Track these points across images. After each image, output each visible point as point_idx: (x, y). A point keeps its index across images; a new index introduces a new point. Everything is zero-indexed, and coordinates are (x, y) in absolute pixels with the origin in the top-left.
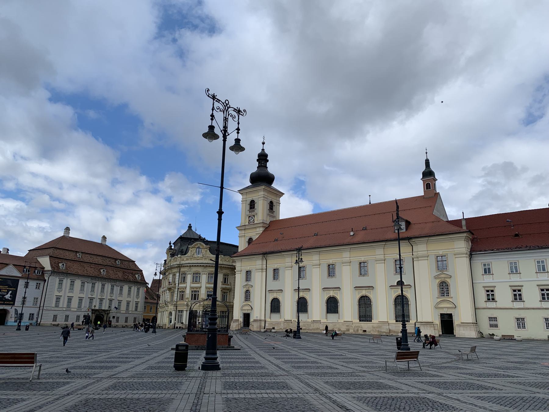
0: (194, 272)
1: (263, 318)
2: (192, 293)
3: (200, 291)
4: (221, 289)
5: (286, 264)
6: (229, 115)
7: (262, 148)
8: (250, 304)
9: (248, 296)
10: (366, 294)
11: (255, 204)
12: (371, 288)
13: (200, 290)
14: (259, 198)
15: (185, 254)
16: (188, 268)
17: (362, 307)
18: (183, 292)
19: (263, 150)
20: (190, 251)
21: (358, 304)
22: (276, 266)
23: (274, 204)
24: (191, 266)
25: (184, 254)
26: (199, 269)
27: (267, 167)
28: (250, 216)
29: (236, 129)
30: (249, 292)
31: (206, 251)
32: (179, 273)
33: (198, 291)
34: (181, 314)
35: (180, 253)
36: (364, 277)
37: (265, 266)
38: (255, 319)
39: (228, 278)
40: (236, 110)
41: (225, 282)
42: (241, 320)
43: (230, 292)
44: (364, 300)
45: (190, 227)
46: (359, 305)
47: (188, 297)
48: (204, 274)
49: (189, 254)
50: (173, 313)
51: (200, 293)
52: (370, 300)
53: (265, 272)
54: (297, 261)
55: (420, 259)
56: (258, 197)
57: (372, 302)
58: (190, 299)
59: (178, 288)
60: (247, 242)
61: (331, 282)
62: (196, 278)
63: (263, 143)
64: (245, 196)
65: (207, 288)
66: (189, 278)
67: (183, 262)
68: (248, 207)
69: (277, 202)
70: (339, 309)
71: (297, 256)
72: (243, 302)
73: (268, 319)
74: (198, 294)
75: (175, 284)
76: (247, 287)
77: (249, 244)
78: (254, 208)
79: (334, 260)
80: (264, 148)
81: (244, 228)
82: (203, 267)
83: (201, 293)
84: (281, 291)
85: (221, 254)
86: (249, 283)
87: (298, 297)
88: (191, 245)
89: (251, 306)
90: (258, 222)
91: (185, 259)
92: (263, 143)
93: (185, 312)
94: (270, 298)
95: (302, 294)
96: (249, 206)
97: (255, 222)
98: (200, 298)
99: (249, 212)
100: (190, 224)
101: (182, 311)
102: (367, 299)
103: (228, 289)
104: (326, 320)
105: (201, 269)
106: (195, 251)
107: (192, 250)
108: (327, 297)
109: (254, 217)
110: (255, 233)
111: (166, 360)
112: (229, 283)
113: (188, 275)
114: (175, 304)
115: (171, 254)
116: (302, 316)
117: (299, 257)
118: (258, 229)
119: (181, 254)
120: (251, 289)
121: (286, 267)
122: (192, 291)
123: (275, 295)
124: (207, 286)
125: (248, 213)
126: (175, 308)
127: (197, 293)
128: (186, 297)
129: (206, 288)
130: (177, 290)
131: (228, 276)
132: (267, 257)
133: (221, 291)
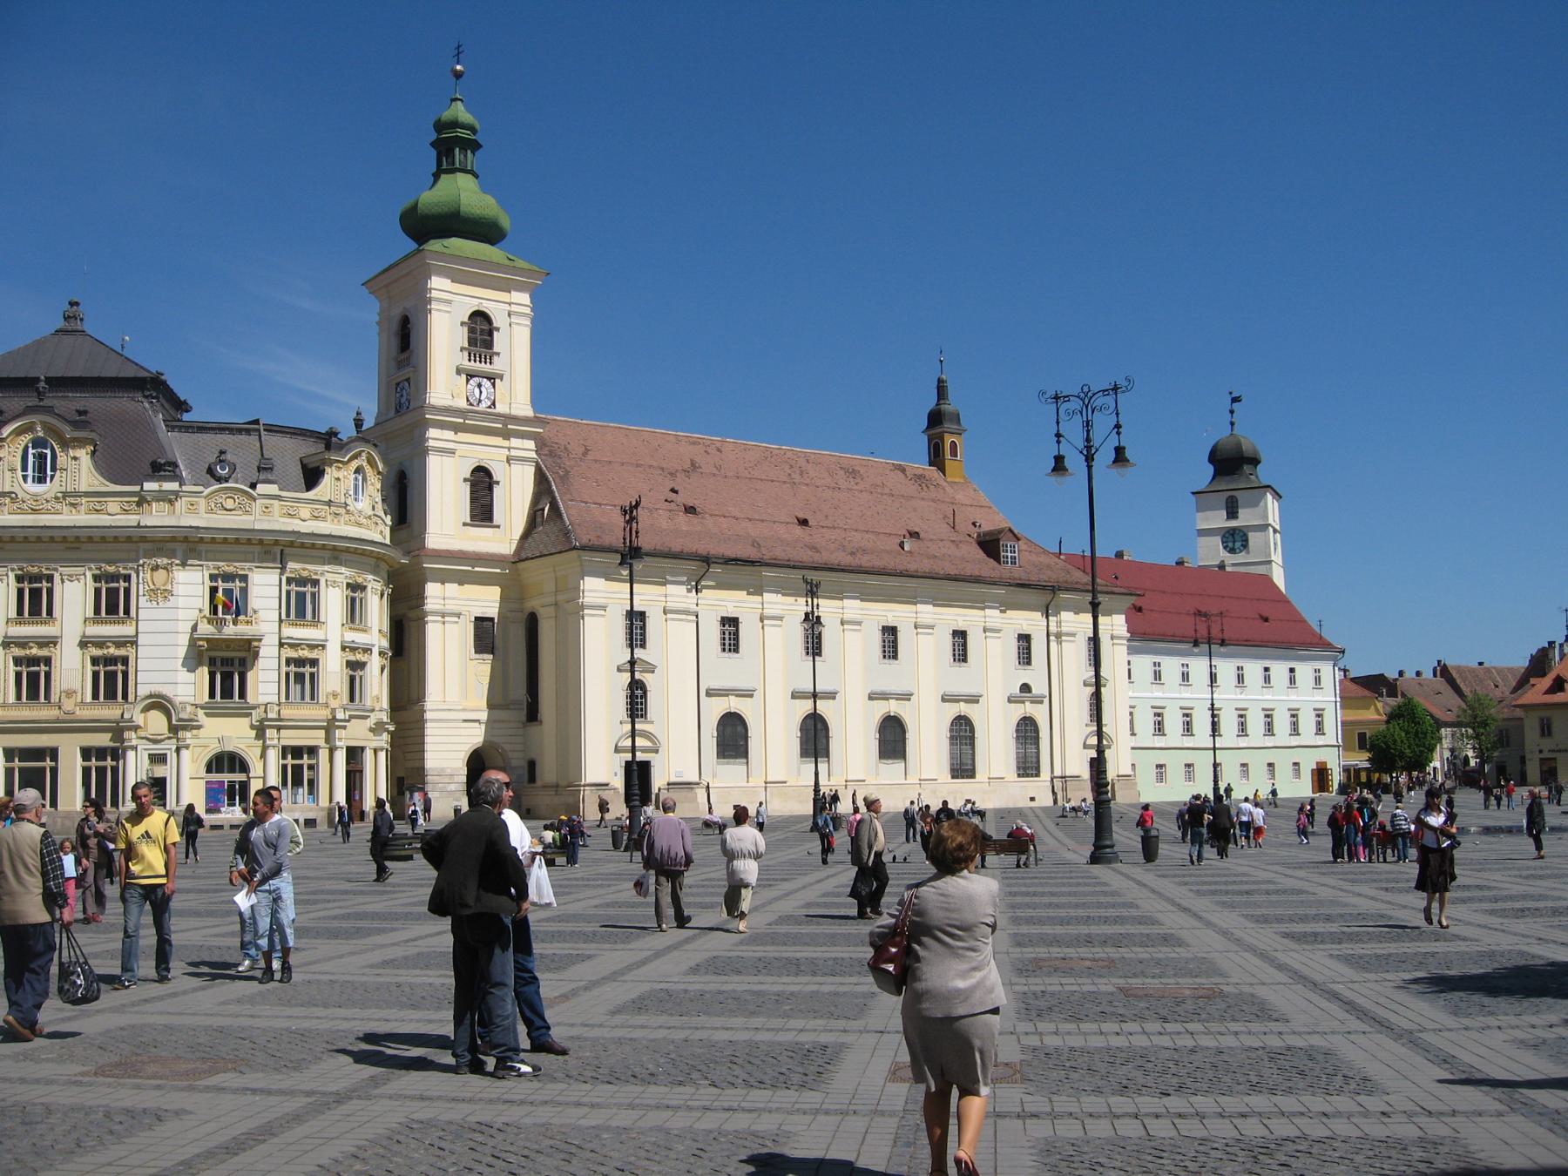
1: (696, 779)
11: (495, 333)
12: (974, 700)
38: (673, 779)
42: (619, 783)
46: (953, 739)
55: (1063, 638)
59: (281, 645)
61: (891, 676)
66: (333, 601)
83: (374, 673)
94: (716, 709)
96: (466, 329)
99: (466, 354)
107: (341, 474)
109: (494, 385)
111: (783, 929)
118: (515, 442)
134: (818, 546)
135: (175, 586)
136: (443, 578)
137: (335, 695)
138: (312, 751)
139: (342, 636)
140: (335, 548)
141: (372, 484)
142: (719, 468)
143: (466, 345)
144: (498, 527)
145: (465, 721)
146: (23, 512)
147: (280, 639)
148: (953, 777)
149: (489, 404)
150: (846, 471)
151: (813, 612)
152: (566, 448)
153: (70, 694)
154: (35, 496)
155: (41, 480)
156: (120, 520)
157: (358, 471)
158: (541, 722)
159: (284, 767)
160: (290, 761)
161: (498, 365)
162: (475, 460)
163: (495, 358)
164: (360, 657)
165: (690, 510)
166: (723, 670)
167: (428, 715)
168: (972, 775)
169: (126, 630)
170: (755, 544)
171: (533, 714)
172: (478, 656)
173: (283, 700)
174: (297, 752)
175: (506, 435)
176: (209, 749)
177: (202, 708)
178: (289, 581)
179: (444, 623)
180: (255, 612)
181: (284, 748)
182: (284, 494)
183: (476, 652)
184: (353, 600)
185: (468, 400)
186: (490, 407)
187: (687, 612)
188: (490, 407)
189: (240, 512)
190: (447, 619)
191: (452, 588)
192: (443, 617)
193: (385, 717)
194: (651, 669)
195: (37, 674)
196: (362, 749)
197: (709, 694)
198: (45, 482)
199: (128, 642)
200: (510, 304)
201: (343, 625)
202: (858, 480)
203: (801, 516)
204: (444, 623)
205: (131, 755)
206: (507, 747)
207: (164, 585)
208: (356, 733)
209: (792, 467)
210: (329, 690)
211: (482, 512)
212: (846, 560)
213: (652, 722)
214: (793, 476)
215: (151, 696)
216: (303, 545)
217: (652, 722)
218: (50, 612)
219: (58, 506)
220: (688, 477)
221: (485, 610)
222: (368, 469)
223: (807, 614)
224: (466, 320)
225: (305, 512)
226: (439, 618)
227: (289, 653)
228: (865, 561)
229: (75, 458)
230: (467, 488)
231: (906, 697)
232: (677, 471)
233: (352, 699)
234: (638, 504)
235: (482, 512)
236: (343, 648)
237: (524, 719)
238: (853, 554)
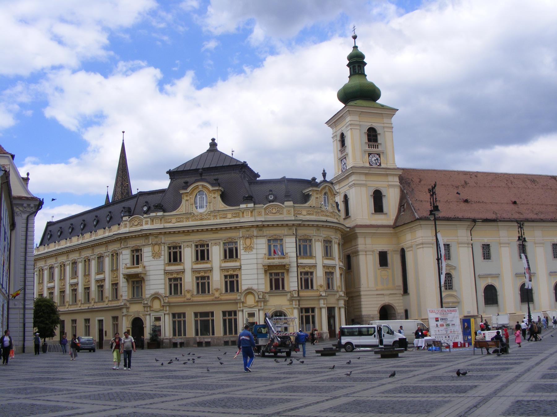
0: (325, 238)
1: (476, 314)
7: (354, 45)
8: (454, 293)
11: (379, 137)
14: (384, 127)
16: (315, 229)
19: (355, 47)
22: (486, 241)
28: (371, 154)
32: (296, 238)
34: (307, 314)
45: (213, 144)
53: (471, 248)
56: (383, 125)
59: (298, 266)
60: (371, 195)
63: (355, 37)
64: (356, 118)
66: (318, 248)
78: (376, 140)
80: (356, 45)
81: (367, 172)
90: (389, 167)
92: (355, 37)
97: (383, 166)
100: (213, 140)
109: (380, 156)
110: (387, 183)
118: (390, 178)
120: (453, 273)
123: (490, 281)
129: (340, 268)
134: (521, 212)
135: (255, 245)
136: (365, 235)
137: (321, 286)
138: (313, 309)
139: (323, 262)
140: (317, 226)
141: (332, 199)
142: (477, 183)
143: (367, 141)
144: (386, 214)
145: (377, 295)
146: (197, 220)
147: (297, 265)
149: (378, 164)
150: (531, 180)
151: (522, 236)
152: (412, 180)
153: (217, 290)
154: (201, 214)
155: (201, 207)
156: (232, 220)
157: (325, 194)
158: (409, 294)
159: (302, 317)
160: (304, 314)
161: (380, 149)
162: (373, 188)
163: (379, 146)
164: (330, 270)
165: (466, 201)
166: (484, 267)
167: (362, 293)
169: (236, 264)
170: (494, 213)
171: (406, 291)
172: (381, 268)
173: (300, 289)
174: (307, 310)
175: (387, 175)
176: (271, 310)
177: (267, 293)
179: (366, 255)
180: (287, 254)
181: (302, 309)
182: (296, 205)
183: (380, 266)
184: (327, 247)
185: (370, 164)
186: (379, 166)
187: (468, 244)
188: (379, 166)
189: (279, 214)
190: (367, 253)
191: (369, 241)
192: (366, 252)
193: (342, 294)
194: (455, 268)
196: (334, 308)
198: (204, 208)
199: (237, 268)
200: (383, 123)
202: (536, 184)
203: (514, 200)
204: (366, 255)
205: (240, 315)
206: (395, 305)
207: (250, 245)
208: (332, 302)
209: (507, 181)
210: (319, 284)
211: (378, 207)
212: (534, 217)
213: (456, 291)
214: (508, 184)
215: (247, 289)
216: (304, 225)
217: (456, 291)
218: (208, 259)
219: (209, 217)
220: (464, 188)
221: (383, 248)
223: (519, 237)
224: (366, 131)
225: (304, 212)
226: (365, 253)
227: (301, 270)
228: (542, 216)
229: (214, 198)
232: (459, 186)
233: (329, 287)
234: (435, 186)
235: (378, 207)
236: (324, 266)
237: (402, 292)
238: (537, 214)
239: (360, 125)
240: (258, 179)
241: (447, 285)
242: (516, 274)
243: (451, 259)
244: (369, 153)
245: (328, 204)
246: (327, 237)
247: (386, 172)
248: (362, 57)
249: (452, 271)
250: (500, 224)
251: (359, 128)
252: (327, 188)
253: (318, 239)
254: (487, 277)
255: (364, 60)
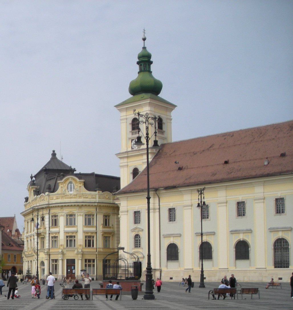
0: (67, 213)
2: (67, 239)
3: (77, 237)
4: (102, 233)
5: (184, 202)
6: (149, 124)
9: (138, 241)
10: (283, 236)
13: (77, 235)
15: (53, 192)
16: (59, 208)
17: (278, 252)
18: (55, 237)
20: (60, 188)
21: (273, 248)
22: (171, 206)
23: (164, 121)
24: (62, 206)
25: (52, 190)
26: (75, 211)
27: (151, 72)
29: (154, 133)
30: (139, 237)
31: (80, 187)
32: (49, 215)
33: (74, 237)
34: (56, 263)
35: (48, 190)
36: (281, 216)
37: (158, 204)
39: (109, 220)
40: (153, 118)
41: (106, 225)
43: (113, 236)
44: (281, 243)
46: (276, 249)
47: (63, 244)
48: (80, 215)
49: (59, 191)
50: (46, 263)
51: (77, 238)
52: (288, 243)
53: (158, 213)
54: (199, 204)
57: (289, 244)
58: (65, 246)
59: (49, 234)
60: (131, 173)
61: (241, 223)
62: (71, 220)
65: (84, 232)
66: (62, 221)
67: (54, 201)
68: (130, 128)
69: (167, 119)
70: (250, 255)
71: (199, 199)
72: (133, 249)
73: (164, 269)
74: (75, 240)
75: (45, 229)
76: (137, 230)
77: (134, 177)
79: (244, 196)
81: (126, 155)
82: (77, 208)
84: (180, 235)
85: (99, 190)
86: (138, 226)
87: (201, 241)
88: (61, 179)
89: (142, 253)
91: (54, 198)
93: (60, 263)
95: (205, 239)
98: (77, 245)
99: (131, 133)
101: (56, 261)
102: (284, 242)
103: (110, 233)
104: (235, 267)
105: (75, 209)
106: (66, 187)
108: (236, 241)
112: (111, 225)
113: (60, 218)
114: (47, 252)
115: (34, 191)
116: (207, 264)
117: (201, 200)
119: (49, 191)
121: (184, 206)
122: (67, 237)
123: (172, 240)
124: (84, 230)
125: (130, 136)
126: (48, 256)
127: (73, 239)
128: (60, 244)
129: (84, 232)
130: (47, 235)
131: (109, 216)
132: (159, 193)
133: (102, 235)
140: (58, 206)
148: (275, 267)
162: (133, 167)
168: (288, 267)
178: (52, 216)
181: (53, 260)
185: (132, 148)
195: (90, 240)
197: (166, 236)
201: (64, 226)
208: (70, 255)
222: (73, 182)
230: (132, 176)
231: (250, 231)
239: (127, 119)
240: (75, 172)
241: (138, 243)
242: (180, 236)
243: (141, 223)
244: (132, 140)
245: (74, 189)
246: (69, 212)
247: (139, 152)
248: (149, 56)
249: (140, 232)
250: (180, 189)
251: (125, 121)
252: (70, 179)
253: (62, 215)
254: (170, 237)
255: (151, 60)
